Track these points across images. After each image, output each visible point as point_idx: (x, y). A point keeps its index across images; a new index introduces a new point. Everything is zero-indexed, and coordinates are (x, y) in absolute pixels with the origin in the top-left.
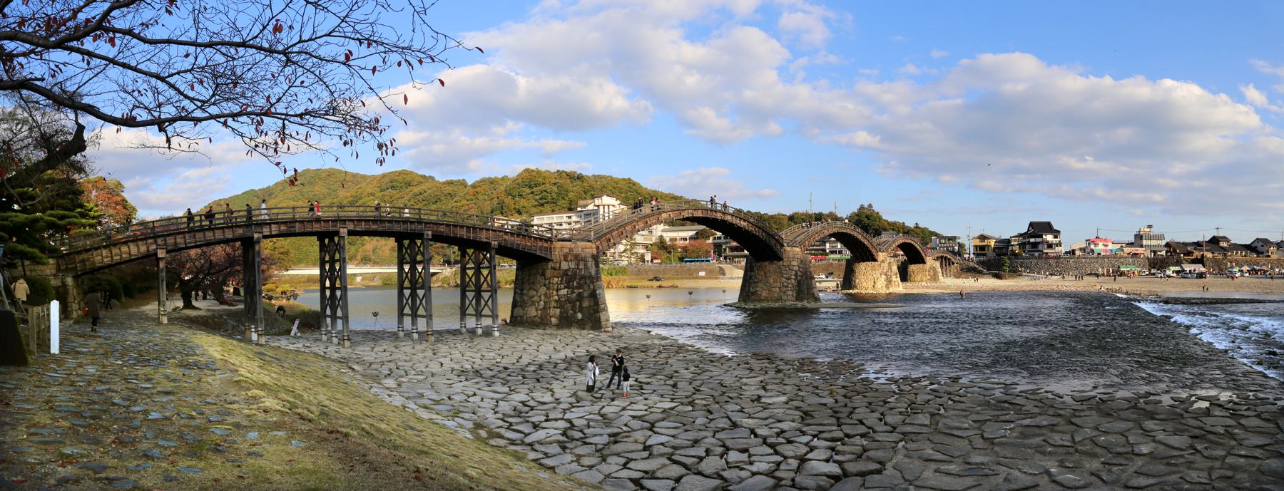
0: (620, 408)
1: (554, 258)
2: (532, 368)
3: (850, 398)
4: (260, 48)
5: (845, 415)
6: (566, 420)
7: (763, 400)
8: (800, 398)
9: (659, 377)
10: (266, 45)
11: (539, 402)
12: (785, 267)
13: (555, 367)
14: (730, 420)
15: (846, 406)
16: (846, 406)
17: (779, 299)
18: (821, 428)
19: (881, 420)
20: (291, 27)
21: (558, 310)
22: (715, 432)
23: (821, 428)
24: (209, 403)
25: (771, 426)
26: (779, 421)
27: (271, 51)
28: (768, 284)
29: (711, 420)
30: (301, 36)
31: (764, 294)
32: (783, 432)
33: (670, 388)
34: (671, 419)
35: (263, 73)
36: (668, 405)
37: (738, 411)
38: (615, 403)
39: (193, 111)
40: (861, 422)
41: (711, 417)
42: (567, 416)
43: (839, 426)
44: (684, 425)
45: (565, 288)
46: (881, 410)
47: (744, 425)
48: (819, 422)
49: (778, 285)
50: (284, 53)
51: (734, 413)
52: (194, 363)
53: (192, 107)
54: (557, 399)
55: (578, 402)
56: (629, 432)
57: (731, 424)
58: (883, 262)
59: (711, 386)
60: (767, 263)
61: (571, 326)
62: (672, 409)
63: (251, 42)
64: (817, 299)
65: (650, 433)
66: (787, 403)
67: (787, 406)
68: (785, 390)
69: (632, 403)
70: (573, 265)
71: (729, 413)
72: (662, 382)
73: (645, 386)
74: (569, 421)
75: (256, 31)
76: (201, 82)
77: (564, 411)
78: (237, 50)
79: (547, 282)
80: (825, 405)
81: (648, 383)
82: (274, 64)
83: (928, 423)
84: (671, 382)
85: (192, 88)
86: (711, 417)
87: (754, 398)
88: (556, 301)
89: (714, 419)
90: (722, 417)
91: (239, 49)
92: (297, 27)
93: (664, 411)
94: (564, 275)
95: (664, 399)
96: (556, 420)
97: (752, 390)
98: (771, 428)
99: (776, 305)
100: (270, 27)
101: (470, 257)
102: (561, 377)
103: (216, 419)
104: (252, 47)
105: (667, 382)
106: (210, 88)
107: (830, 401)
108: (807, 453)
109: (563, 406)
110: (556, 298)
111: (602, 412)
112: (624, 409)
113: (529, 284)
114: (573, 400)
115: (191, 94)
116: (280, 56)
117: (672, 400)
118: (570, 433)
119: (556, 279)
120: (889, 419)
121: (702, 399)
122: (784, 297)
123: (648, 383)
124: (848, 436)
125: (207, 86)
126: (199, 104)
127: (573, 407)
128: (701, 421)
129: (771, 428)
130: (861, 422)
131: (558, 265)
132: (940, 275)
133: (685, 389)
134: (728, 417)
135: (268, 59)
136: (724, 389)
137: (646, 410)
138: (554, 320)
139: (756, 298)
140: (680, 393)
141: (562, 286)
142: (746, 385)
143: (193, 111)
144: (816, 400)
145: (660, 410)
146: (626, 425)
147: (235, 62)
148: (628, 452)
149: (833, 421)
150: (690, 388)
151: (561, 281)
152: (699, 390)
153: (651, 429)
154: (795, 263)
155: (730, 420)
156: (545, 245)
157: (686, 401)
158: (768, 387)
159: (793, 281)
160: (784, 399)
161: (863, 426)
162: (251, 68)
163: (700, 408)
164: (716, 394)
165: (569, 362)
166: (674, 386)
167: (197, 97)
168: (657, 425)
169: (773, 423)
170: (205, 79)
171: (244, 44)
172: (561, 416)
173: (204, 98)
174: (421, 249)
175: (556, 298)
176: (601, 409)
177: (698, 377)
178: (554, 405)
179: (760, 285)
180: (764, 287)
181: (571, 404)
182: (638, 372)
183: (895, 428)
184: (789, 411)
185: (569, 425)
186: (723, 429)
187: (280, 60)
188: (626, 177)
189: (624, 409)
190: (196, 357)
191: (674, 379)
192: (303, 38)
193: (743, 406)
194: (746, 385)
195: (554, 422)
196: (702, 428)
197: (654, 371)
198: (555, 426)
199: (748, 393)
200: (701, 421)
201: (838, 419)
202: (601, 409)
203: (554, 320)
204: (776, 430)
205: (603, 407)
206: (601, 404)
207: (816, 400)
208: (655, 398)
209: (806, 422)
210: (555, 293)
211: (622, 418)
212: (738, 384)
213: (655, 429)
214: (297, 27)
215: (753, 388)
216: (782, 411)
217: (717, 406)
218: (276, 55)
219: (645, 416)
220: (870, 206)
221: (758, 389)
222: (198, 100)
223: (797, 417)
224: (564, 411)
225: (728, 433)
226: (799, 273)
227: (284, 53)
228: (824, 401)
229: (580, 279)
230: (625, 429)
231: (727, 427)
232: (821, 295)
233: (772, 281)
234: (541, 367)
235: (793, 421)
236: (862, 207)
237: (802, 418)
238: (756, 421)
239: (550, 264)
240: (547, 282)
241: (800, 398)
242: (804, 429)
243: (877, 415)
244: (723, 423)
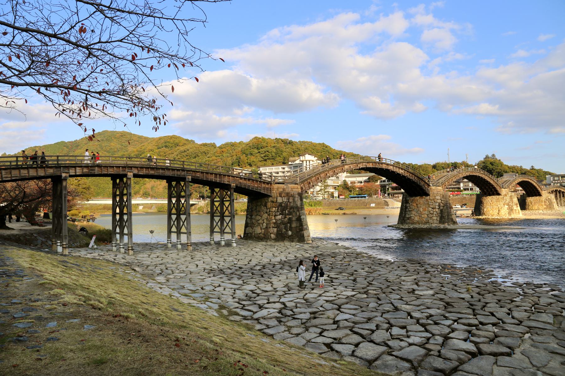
0: (317, 295)
1: (272, 195)
2: (258, 268)
3: (483, 295)
4: (69, 42)
5: (479, 308)
6: (281, 303)
7: (416, 292)
8: (443, 293)
9: (344, 274)
10: (73, 40)
11: (263, 291)
12: (432, 200)
13: (274, 267)
14: (393, 305)
15: (480, 301)
16: (480, 301)
18: (460, 315)
19: (509, 314)
20: (93, 31)
21: (275, 229)
22: (383, 313)
23: (460, 315)
24: (14, 303)
25: (422, 311)
26: (428, 308)
27: (77, 45)
28: (419, 212)
29: (380, 305)
30: (100, 39)
31: (416, 219)
32: (431, 316)
33: (351, 282)
34: (352, 303)
35: (71, 60)
36: (350, 293)
37: (399, 299)
38: (314, 291)
39: (10, 77)
40: (493, 314)
41: (380, 302)
42: (281, 300)
43: (475, 315)
44: (361, 307)
45: (280, 214)
46: (509, 306)
47: (403, 309)
48: (458, 311)
49: (426, 212)
50: (87, 48)
51: (396, 301)
52: (4, 272)
53: (9, 74)
54: (275, 289)
55: (289, 291)
56: (323, 311)
57: (394, 308)
58: (506, 195)
59: (379, 281)
60: (418, 198)
61: (285, 239)
62: (353, 296)
63: (62, 36)
64: (455, 223)
65: (338, 312)
66: (433, 295)
67: (434, 298)
68: (432, 286)
69: (325, 292)
70: (285, 200)
71: (392, 300)
72: (346, 278)
73: (334, 280)
74: (283, 303)
75: (66, 27)
76: (18, 57)
77: (280, 297)
78: (50, 40)
79: (268, 210)
80: (463, 299)
81: (337, 279)
82: (80, 55)
83: (551, 321)
84: (352, 278)
85: (10, 59)
86: (380, 302)
87: (410, 290)
88: (274, 223)
89: (382, 304)
90: (388, 303)
91: (52, 39)
92: (98, 32)
93: (348, 297)
94: (279, 206)
95: (347, 289)
96: (274, 302)
97: (408, 285)
98: (422, 313)
99: (425, 226)
100: (77, 28)
101: (217, 193)
102: (277, 274)
103: (20, 315)
104: (63, 39)
105: (350, 278)
106: (26, 63)
107: (467, 296)
108: (450, 333)
109: (279, 293)
110: (274, 221)
111: (305, 297)
112: (320, 295)
113: (256, 212)
114: (286, 289)
115: (9, 64)
116: (84, 50)
117: (353, 290)
118: (284, 311)
119: (274, 209)
120: (515, 314)
121: (373, 290)
122: (431, 221)
123: (337, 279)
124: (481, 323)
125: (24, 61)
126: (17, 73)
127: (286, 294)
128: (372, 305)
129: (422, 313)
130: (493, 314)
131: (275, 199)
132: (555, 205)
133: (362, 283)
134: (391, 303)
135: (76, 50)
136: (389, 284)
137: (335, 297)
138: (273, 236)
139: (410, 222)
140: (358, 285)
141: (278, 213)
142: (404, 281)
143: (10, 77)
144: (456, 295)
145: (345, 297)
146: (321, 306)
147: (49, 48)
148: (323, 325)
149: (470, 311)
150: (365, 282)
151: (277, 210)
152: (371, 284)
153: (338, 310)
154: (438, 197)
155: (393, 305)
156: (267, 186)
157: (362, 291)
158: (420, 284)
159: (437, 210)
160: (431, 292)
161: (494, 317)
162: (62, 54)
163: (372, 296)
164: (383, 287)
165: (283, 264)
166: (355, 280)
167: (14, 67)
168: (342, 307)
169: (424, 309)
170: (22, 55)
171: (55, 36)
172: (278, 300)
173: (20, 69)
174: (184, 188)
175: (274, 221)
176: (305, 295)
177: (371, 275)
178: (273, 292)
179: (413, 213)
180: (416, 214)
181: (284, 292)
182: (329, 271)
183: (521, 322)
184: (435, 301)
185: (283, 306)
186: (388, 312)
187: (84, 53)
188: (321, 142)
189: (320, 295)
190: (6, 268)
191: (354, 276)
192: (102, 40)
193: (402, 296)
194: (404, 281)
195: (273, 304)
196: (374, 310)
197: (341, 270)
198: (274, 307)
199: (406, 287)
200: (372, 305)
201: (474, 310)
202: (305, 295)
203: (273, 236)
204: (426, 314)
205: (306, 294)
206: (304, 292)
207: (456, 295)
208: (341, 288)
209: (448, 310)
210: (273, 218)
211: (319, 301)
212: (398, 280)
213: (341, 310)
214: (98, 32)
215: (409, 283)
216: (430, 301)
217: (384, 295)
218: (81, 49)
219: (334, 300)
220: (493, 155)
221: (413, 285)
222: (15, 69)
223: (441, 306)
224: (280, 297)
225: (391, 314)
226: (442, 205)
227: (87, 48)
228: (462, 296)
229: (291, 209)
230: (321, 309)
231: (390, 309)
232: (458, 220)
233: (421, 210)
234: (264, 267)
235: (439, 309)
236: (487, 157)
237: (445, 307)
238: (411, 307)
239: (270, 199)
240: (268, 210)
241: (443, 293)
242: (447, 315)
243: (505, 310)
244: (388, 307)
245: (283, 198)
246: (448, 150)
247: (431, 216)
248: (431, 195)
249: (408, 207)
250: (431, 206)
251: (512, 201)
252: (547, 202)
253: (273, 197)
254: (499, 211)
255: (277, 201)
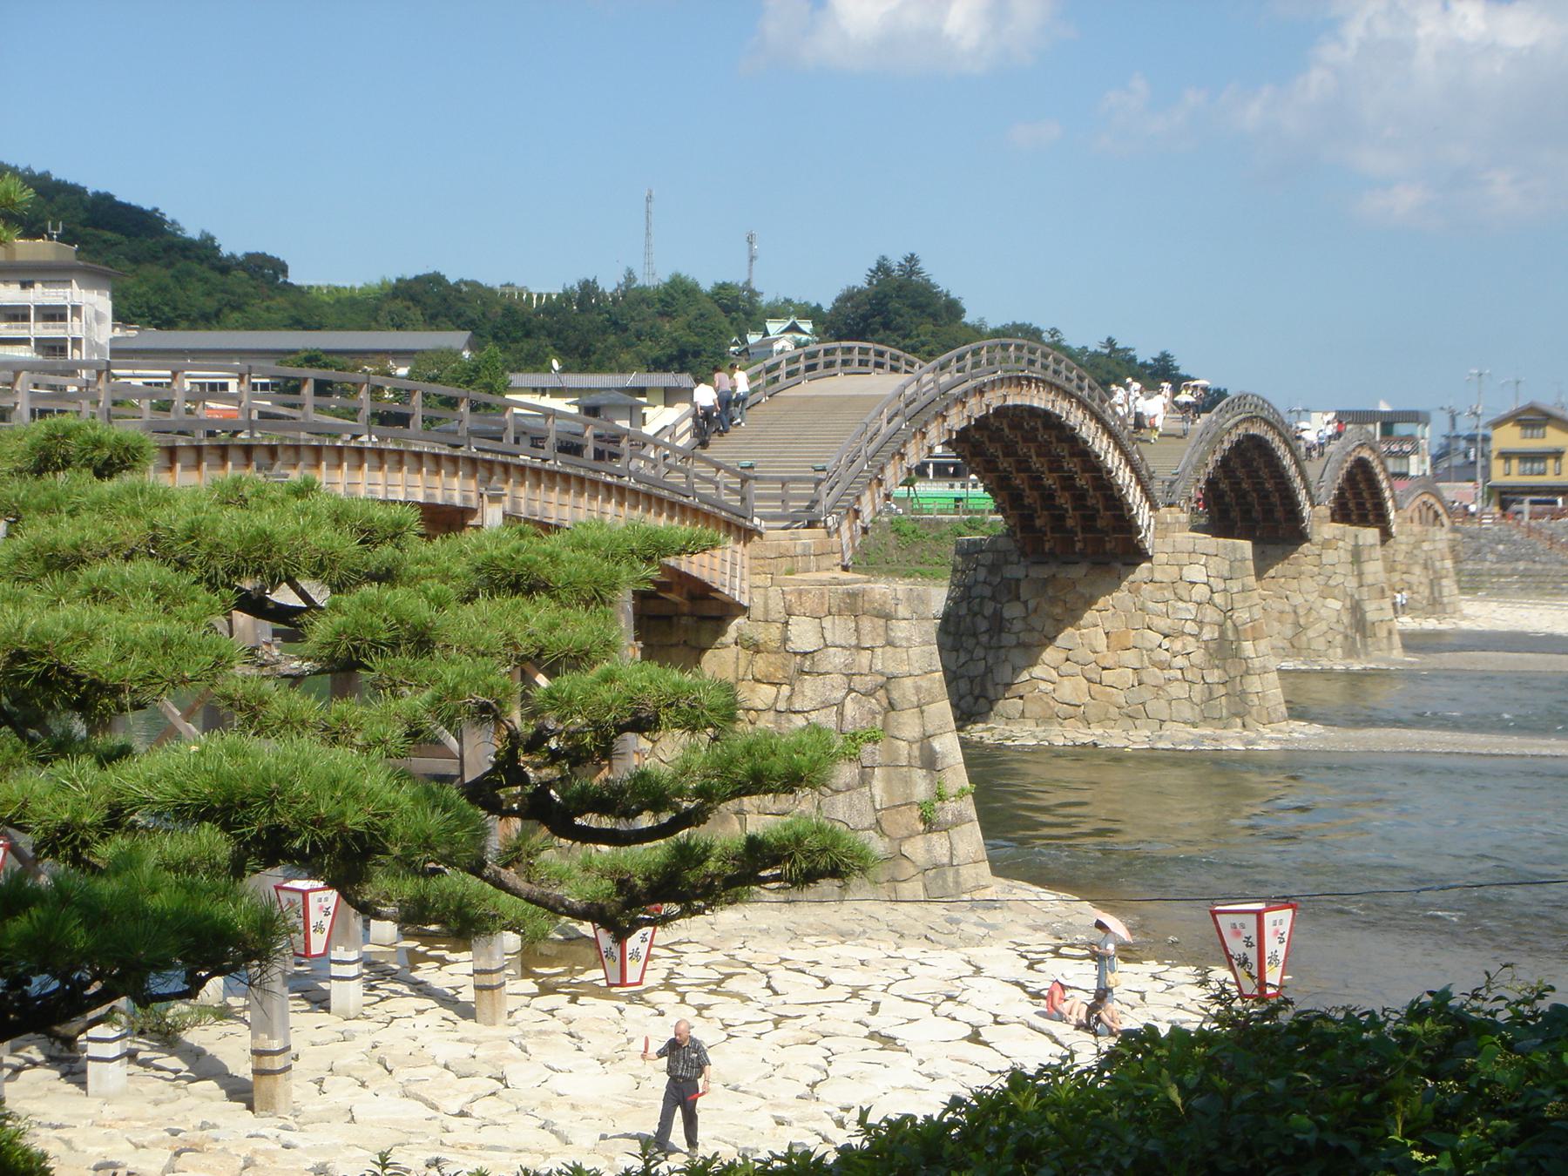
17: (1131, 716)
60: (1078, 572)
119: (765, 694)
122: (1157, 707)
131: (775, 631)
159: (1191, 644)
220: (912, 259)
236: (883, 268)
239: (736, 626)
245: (827, 622)
246: (649, 199)
247: (1154, 675)
248: (1160, 558)
249: (1018, 625)
250: (1163, 624)
251: (1360, 575)
252: (1417, 570)
253: (757, 612)
254: (1297, 624)
255: (785, 640)
